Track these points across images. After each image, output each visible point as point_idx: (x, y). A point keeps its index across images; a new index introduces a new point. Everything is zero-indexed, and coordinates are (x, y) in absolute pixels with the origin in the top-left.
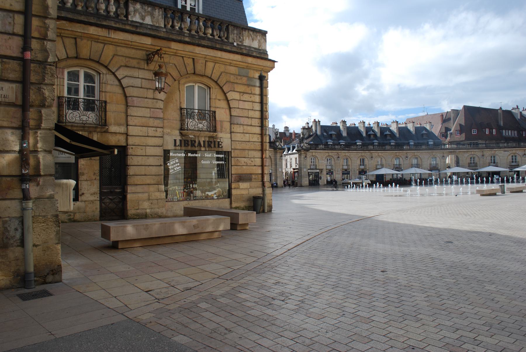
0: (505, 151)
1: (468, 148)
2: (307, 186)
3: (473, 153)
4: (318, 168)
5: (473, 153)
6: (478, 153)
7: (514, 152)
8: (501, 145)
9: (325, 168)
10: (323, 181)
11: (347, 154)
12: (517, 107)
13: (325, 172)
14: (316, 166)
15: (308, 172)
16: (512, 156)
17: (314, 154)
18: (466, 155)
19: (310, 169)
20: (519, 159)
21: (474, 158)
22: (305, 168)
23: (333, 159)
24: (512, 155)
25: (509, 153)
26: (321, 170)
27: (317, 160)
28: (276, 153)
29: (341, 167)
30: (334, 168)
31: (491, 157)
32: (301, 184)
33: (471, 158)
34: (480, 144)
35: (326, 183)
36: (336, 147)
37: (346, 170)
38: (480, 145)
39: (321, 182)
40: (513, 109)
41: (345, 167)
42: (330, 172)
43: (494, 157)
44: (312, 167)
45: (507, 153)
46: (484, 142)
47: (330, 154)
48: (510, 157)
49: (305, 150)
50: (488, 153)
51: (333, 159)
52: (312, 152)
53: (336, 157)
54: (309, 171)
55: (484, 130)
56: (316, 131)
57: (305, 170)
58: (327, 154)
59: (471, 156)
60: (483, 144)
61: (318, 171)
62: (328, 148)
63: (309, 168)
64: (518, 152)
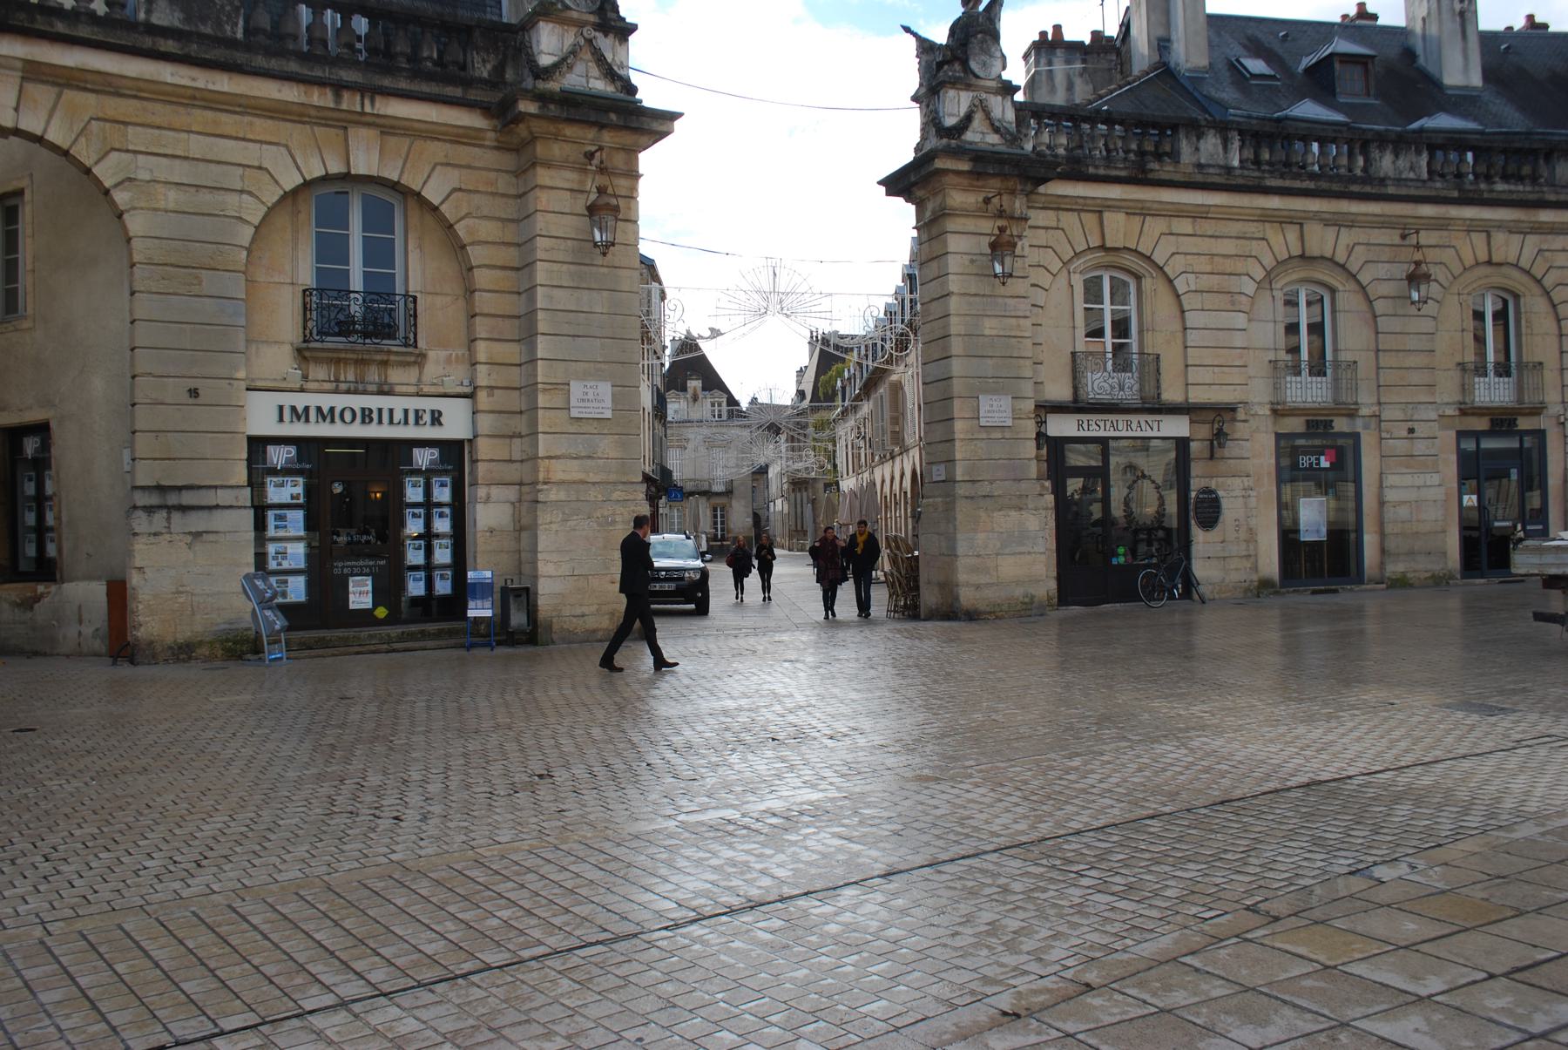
2: (1024, 612)
4: (1171, 394)
9: (1258, 394)
10: (1241, 541)
11: (1506, 247)
13: (1256, 447)
14: (1152, 365)
15: (1055, 448)
17: (1118, 229)
19: (1077, 406)
22: (1001, 384)
23: (1348, 299)
26: (1218, 419)
27: (1161, 307)
28: (521, 155)
29: (1448, 392)
30: (1366, 401)
32: (948, 587)
35: (1270, 562)
36: (1386, 163)
37: (1502, 421)
39: (1213, 558)
41: (1493, 392)
42: (1320, 452)
44: (1099, 384)
47: (1321, 240)
49: (984, 164)
51: (1348, 299)
52: (1100, 209)
53: (1382, 275)
54: (1061, 426)
56: (1162, 44)
57: (996, 409)
58: (1284, 242)
61: (1177, 427)
62: (1287, 167)
63: (1059, 391)
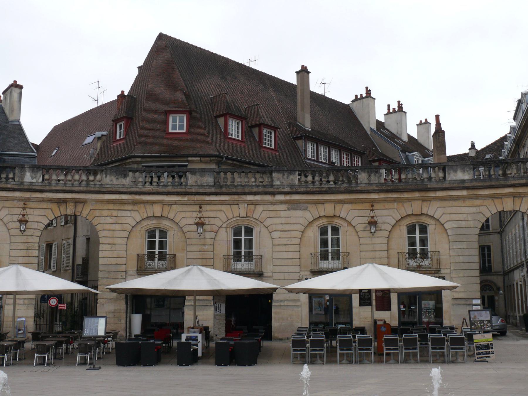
0: (293, 205)
1: (140, 187)
3: (157, 210)
5: (157, 210)
6: (179, 216)
7: (329, 209)
8: (278, 179)
12: (368, 92)
16: (323, 231)
18: (130, 217)
20: (347, 240)
21: (163, 234)
24: (322, 222)
25: (308, 216)
31: (237, 232)
33: (151, 234)
34: (193, 172)
38: (192, 179)
40: (356, 99)
43: (249, 231)
45: (304, 216)
46: (213, 166)
48: (313, 235)
50: (223, 214)
55: (221, 121)
59: (152, 224)
60: (203, 172)
64: (344, 211)
